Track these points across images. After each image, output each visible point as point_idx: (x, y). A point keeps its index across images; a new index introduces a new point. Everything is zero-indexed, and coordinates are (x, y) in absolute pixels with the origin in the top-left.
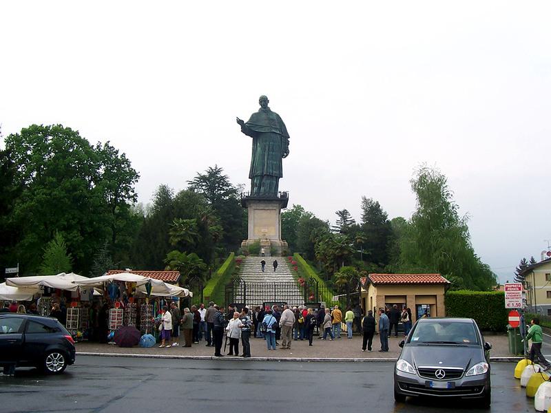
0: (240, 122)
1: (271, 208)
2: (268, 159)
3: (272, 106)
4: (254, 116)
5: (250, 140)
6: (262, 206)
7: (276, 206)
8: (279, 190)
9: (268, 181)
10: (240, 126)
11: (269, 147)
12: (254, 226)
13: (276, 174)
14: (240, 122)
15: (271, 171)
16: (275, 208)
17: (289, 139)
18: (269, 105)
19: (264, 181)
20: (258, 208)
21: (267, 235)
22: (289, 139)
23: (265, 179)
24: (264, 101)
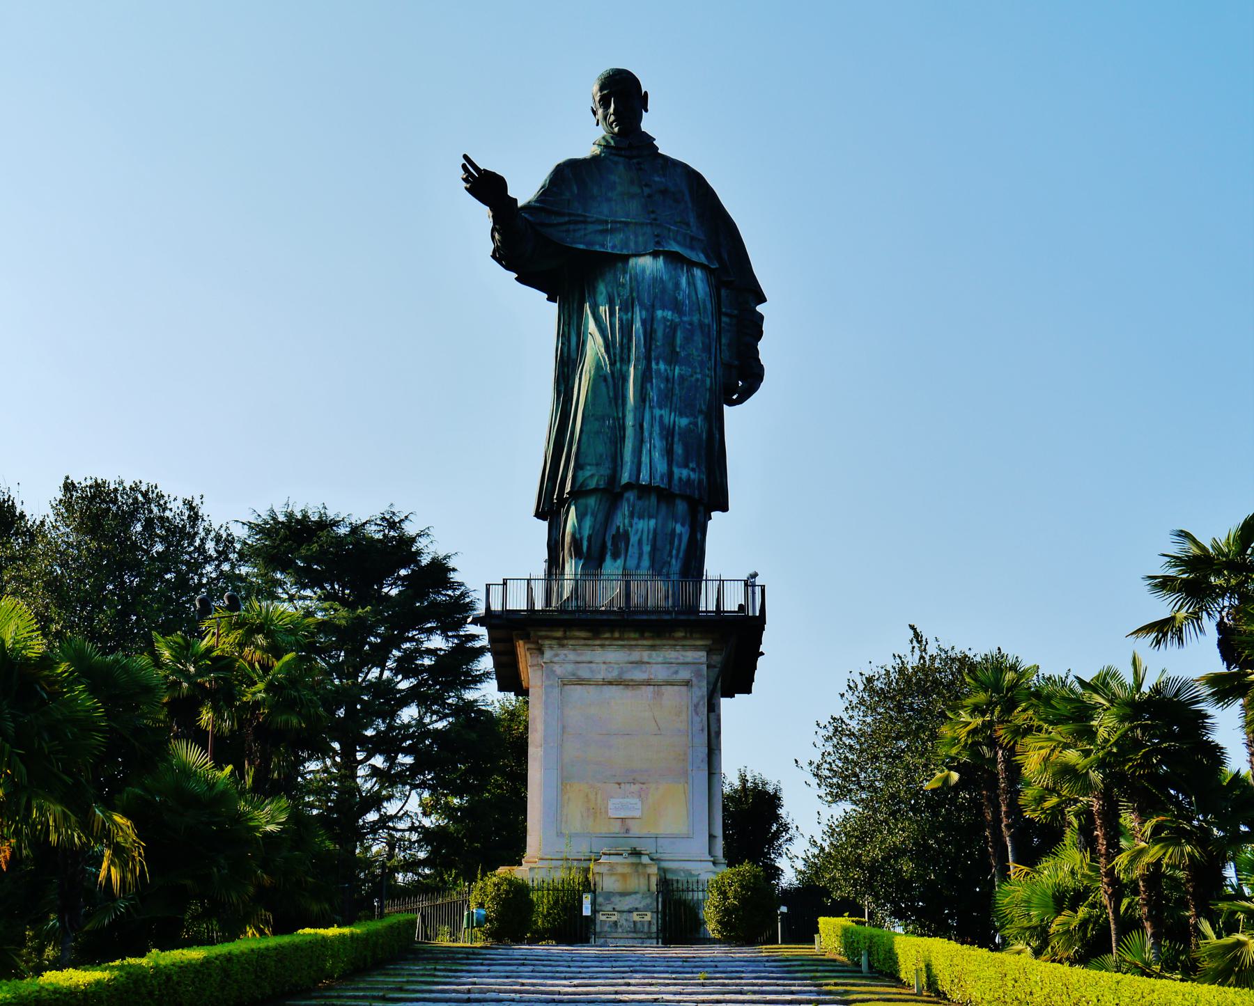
0: (485, 186)
1: (660, 673)
2: (642, 397)
3: (665, 129)
4: (568, 175)
5: (539, 312)
6: (609, 658)
7: (689, 659)
8: (712, 567)
9: (643, 527)
10: (482, 216)
11: (649, 335)
12: (564, 779)
13: (704, 489)
14: (485, 186)
15: (661, 467)
16: (685, 674)
17: (759, 308)
18: (649, 124)
19: (621, 519)
20: (584, 673)
21: (636, 830)
22: (759, 308)
23: (625, 508)
24: (622, 95)
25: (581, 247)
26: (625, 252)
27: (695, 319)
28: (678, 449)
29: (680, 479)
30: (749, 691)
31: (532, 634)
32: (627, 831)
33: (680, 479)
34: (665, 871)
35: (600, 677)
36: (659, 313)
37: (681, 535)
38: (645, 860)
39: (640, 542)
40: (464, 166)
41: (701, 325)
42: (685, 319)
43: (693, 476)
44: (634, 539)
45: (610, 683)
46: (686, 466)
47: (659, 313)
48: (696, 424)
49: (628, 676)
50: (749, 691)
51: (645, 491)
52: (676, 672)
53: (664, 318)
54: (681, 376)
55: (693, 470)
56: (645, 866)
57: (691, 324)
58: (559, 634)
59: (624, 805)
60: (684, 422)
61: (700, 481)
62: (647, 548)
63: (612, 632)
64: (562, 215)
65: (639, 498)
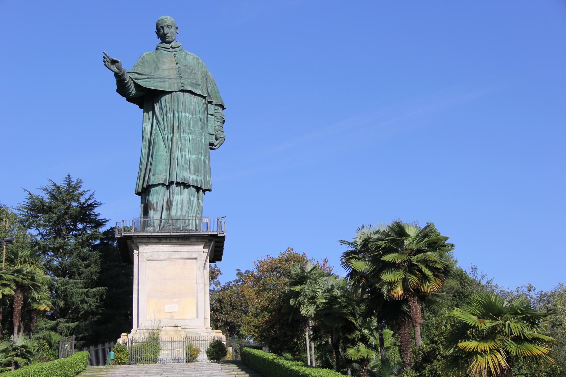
1: (186, 255)
16: (195, 256)
25: (152, 88)
26: (170, 90)
27: (198, 116)
28: (192, 168)
29: (193, 179)
30: (220, 260)
31: (134, 241)
32: (173, 317)
33: (193, 179)
34: (188, 332)
35: (161, 257)
36: (183, 114)
37: (193, 201)
38: (179, 328)
39: (177, 204)
40: (104, 57)
41: (201, 119)
42: (194, 116)
43: (199, 178)
44: (174, 203)
45: (166, 259)
46: (195, 174)
47: (183, 114)
48: (199, 158)
49: (172, 257)
50: (220, 260)
51: (178, 184)
52: (191, 255)
53: (186, 117)
54: (193, 139)
55: (198, 176)
56: (179, 331)
57: (196, 118)
58: (145, 241)
59: (171, 307)
60: (194, 157)
61: (201, 180)
62: (180, 206)
63: (166, 240)
64: (145, 75)
65: (177, 186)
